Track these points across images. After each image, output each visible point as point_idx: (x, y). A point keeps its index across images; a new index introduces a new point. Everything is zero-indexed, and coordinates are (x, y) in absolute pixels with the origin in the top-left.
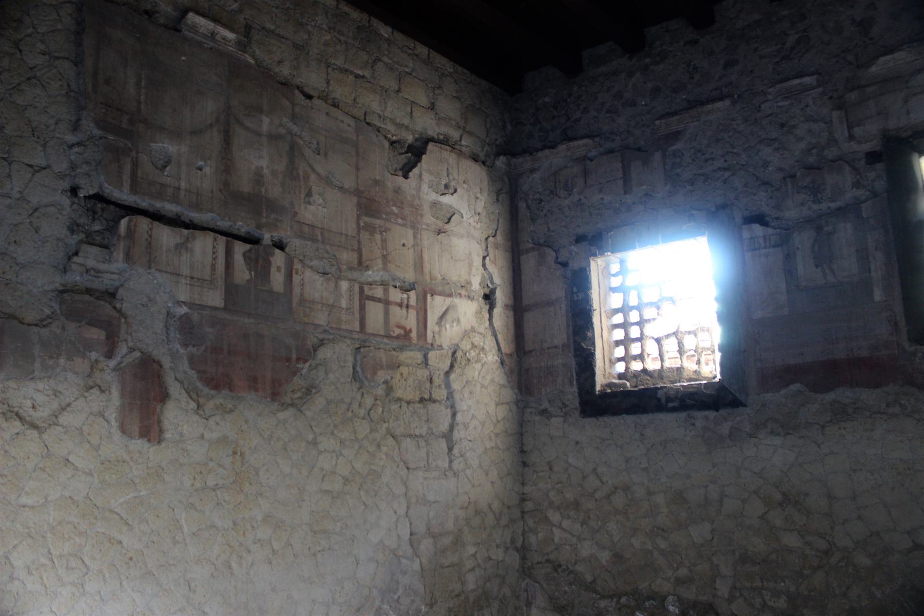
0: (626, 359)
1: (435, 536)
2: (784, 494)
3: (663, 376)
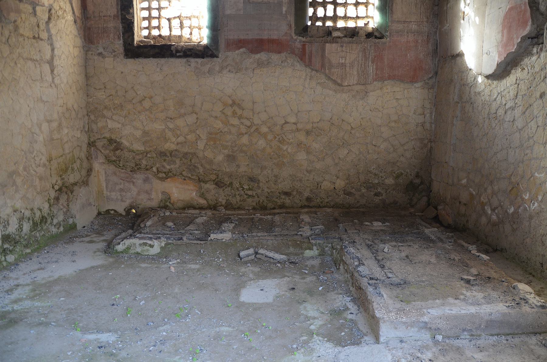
0: (150, 28)
1: (49, 122)
2: (233, 100)
3: (171, 39)
